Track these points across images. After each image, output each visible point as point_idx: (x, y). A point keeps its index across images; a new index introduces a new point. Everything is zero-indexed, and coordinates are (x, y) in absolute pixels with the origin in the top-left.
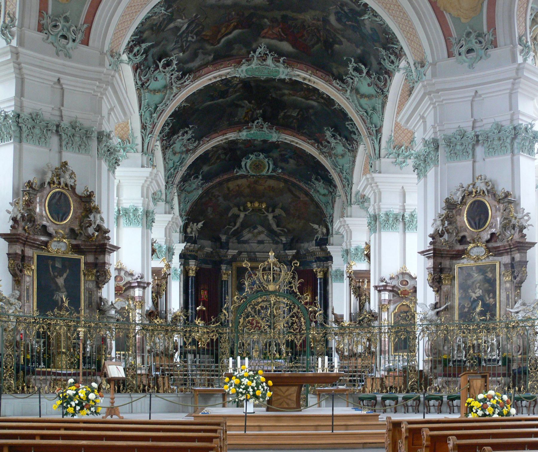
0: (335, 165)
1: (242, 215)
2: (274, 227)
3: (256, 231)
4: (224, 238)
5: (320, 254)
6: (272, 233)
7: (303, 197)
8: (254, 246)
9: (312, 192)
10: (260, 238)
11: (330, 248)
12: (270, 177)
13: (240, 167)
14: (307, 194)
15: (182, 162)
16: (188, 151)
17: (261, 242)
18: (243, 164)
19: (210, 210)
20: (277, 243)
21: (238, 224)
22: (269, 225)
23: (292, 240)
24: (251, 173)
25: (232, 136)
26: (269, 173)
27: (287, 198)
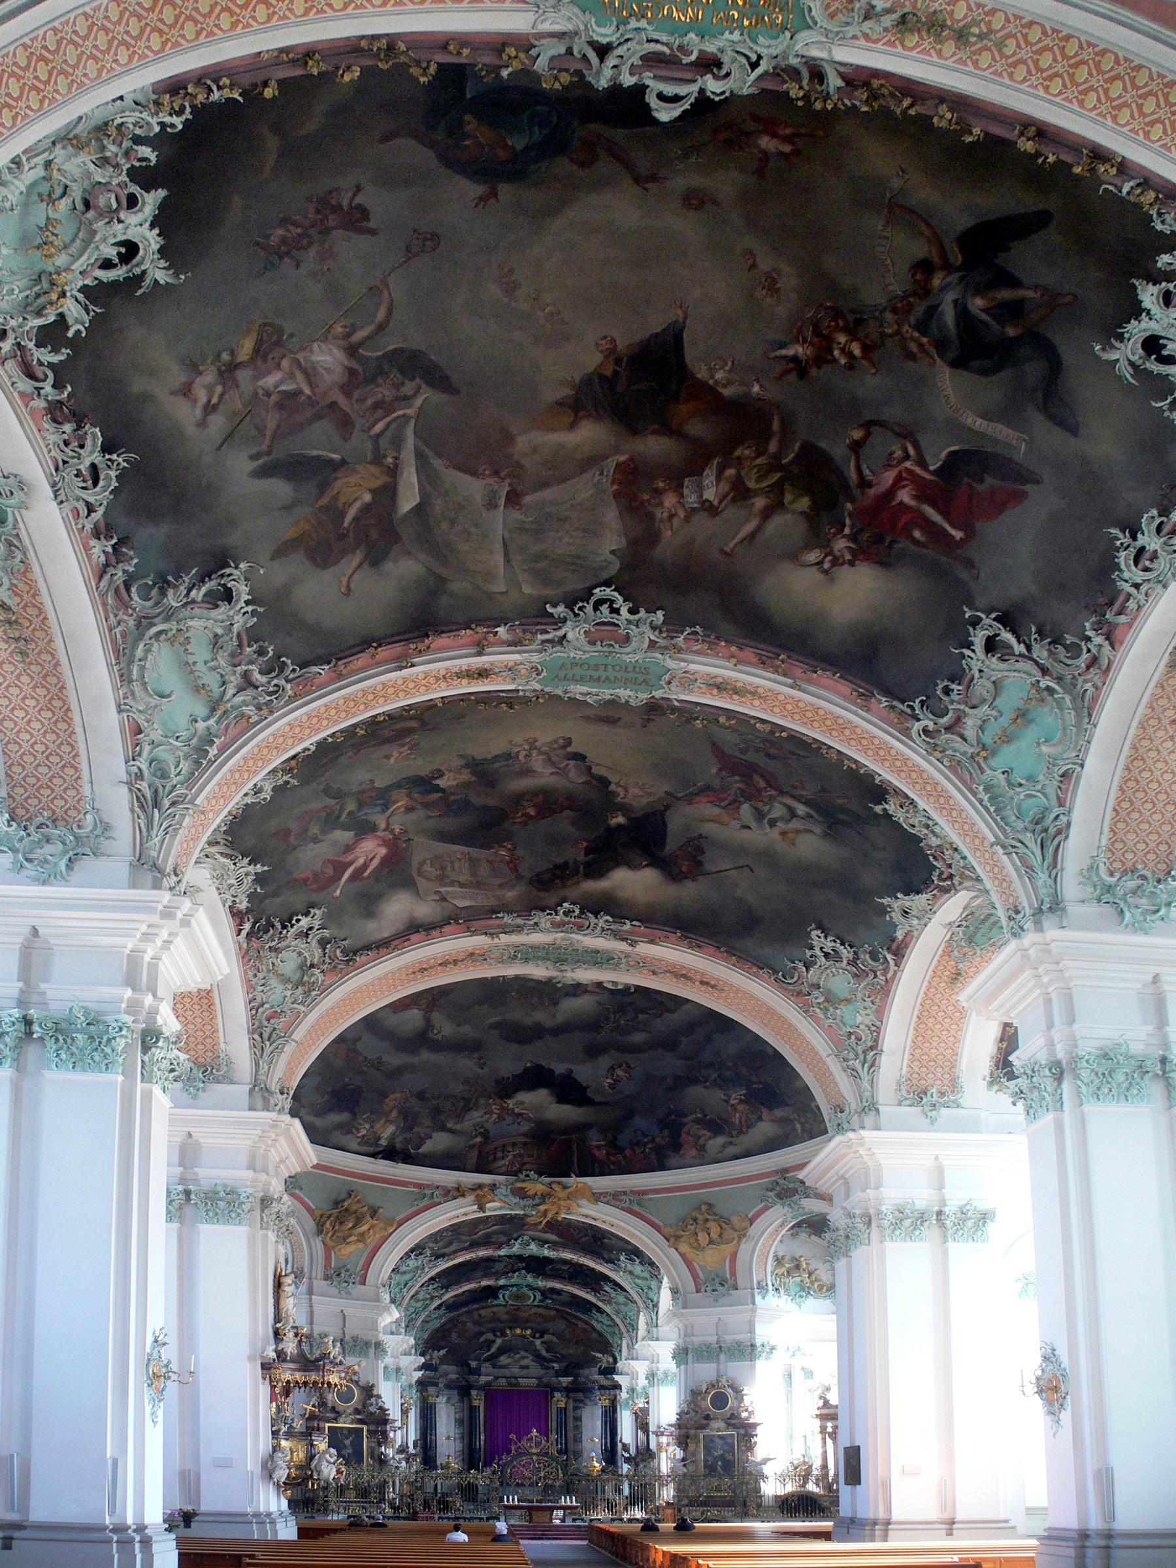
1: (499, 1341)
2: (544, 1353)
3: (517, 1356)
6: (538, 1357)
7: (581, 1324)
8: (516, 1371)
11: (616, 1377)
12: (538, 1306)
13: (496, 1297)
14: (586, 1323)
17: (527, 1367)
18: (501, 1296)
20: (547, 1368)
21: (493, 1350)
22: (536, 1350)
23: (567, 1367)
24: (510, 1302)
26: (536, 1303)
27: (561, 1325)
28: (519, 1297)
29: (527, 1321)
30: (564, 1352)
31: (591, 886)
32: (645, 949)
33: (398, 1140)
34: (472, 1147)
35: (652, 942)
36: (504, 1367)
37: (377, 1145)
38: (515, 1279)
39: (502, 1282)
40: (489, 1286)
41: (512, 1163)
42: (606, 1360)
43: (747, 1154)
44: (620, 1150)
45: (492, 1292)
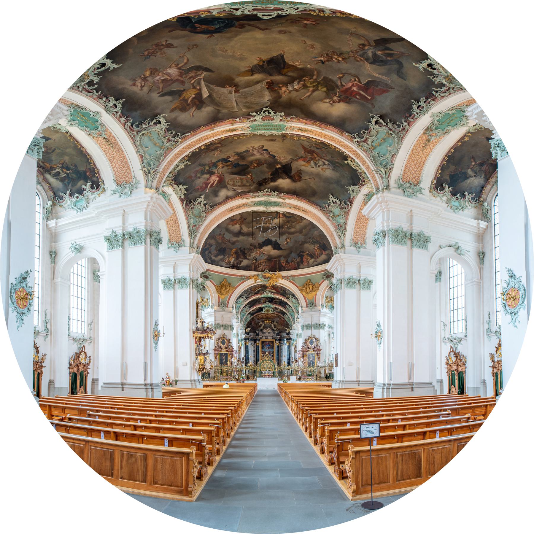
0: (290, 314)
4: (257, 332)
5: (288, 338)
7: (282, 319)
8: (267, 334)
9: (285, 318)
10: (269, 332)
13: (262, 311)
14: (284, 318)
15: (245, 314)
16: (247, 311)
19: (253, 323)
20: (274, 333)
21: (262, 327)
25: (259, 306)
27: (278, 319)
28: (268, 311)
29: (270, 318)
30: (278, 328)
31: (272, 184)
32: (287, 201)
33: (235, 262)
34: (253, 263)
35: (289, 199)
36: (264, 333)
37: (230, 264)
38: (266, 305)
39: (263, 306)
40: (260, 308)
41: (262, 268)
42: (288, 330)
43: (319, 264)
44: (289, 263)
45: (261, 309)
